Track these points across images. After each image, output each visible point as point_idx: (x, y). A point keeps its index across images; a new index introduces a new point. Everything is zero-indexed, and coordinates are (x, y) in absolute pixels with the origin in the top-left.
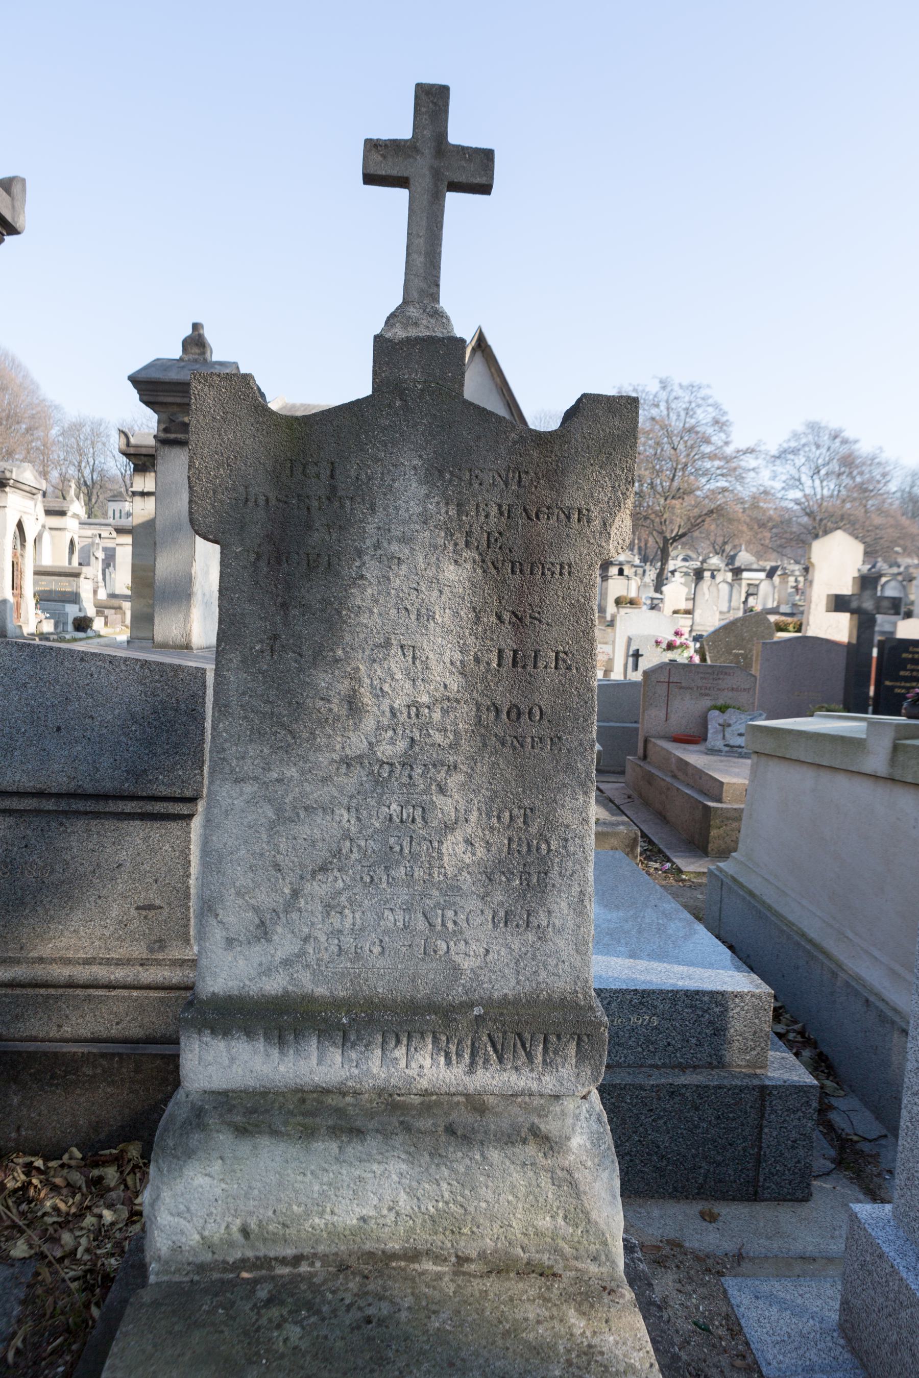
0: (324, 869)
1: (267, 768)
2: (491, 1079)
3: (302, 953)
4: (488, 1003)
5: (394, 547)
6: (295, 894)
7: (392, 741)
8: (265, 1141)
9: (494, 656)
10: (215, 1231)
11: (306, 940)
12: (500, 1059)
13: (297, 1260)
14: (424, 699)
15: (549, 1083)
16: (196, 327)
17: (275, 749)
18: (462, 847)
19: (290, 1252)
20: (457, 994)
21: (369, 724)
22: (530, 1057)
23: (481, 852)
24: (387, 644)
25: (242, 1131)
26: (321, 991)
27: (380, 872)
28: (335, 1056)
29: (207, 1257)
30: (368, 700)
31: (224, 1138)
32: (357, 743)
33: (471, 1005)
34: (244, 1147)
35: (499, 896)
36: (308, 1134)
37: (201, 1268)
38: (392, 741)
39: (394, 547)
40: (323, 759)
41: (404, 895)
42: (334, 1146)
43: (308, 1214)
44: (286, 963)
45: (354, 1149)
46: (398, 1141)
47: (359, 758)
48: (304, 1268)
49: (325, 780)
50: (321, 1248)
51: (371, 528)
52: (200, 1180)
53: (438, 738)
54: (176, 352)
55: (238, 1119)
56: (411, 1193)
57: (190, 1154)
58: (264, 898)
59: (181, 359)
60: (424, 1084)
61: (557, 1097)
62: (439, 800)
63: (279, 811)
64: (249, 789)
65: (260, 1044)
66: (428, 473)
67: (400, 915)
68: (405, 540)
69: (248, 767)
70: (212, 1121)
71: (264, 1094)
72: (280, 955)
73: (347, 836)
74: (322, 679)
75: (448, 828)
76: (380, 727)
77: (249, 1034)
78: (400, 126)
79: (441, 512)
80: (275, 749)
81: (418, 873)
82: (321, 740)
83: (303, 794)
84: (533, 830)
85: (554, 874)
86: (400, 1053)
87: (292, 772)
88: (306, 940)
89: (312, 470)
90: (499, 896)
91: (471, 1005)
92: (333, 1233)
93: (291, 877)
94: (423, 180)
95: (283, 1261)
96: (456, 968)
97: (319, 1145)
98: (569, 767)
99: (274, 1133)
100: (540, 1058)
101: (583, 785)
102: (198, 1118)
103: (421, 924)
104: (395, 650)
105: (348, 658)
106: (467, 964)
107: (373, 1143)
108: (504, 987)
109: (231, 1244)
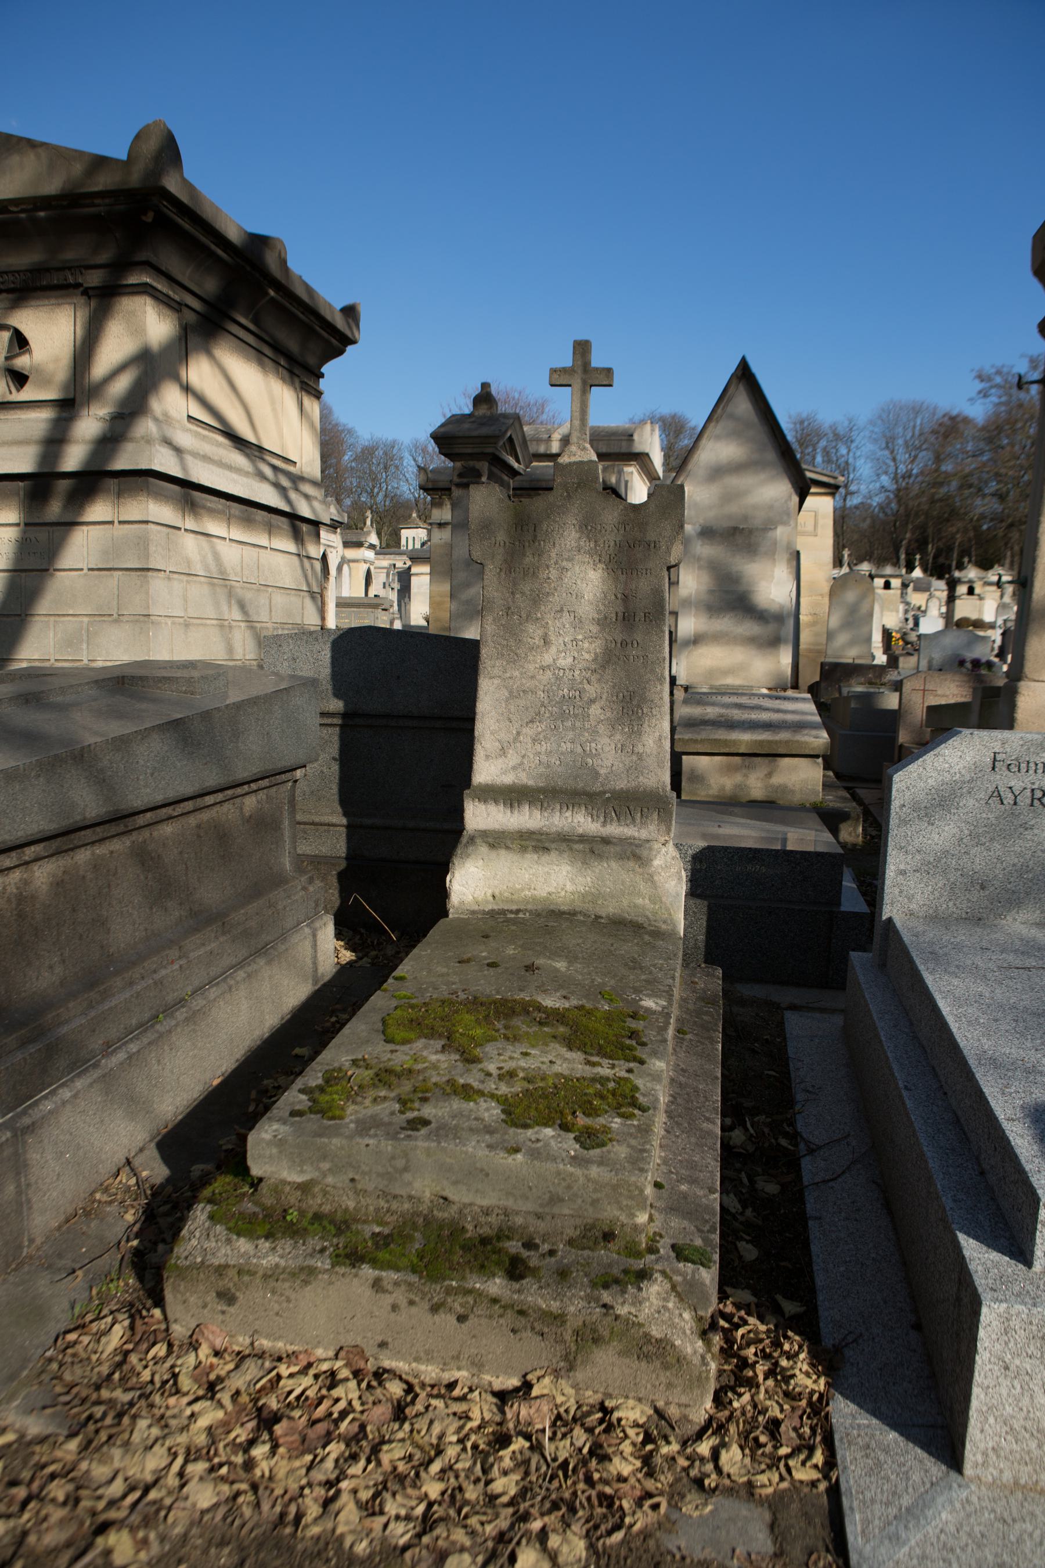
0: (532, 721)
1: (505, 672)
2: (614, 830)
3: (522, 763)
4: (613, 792)
5: (565, 563)
6: (518, 733)
7: (565, 658)
8: (503, 852)
9: (614, 615)
10: (480, 895)
11: (523, 757)
12: (619, 820)
13: (518, 911)
14: (580, 637)
15: (643, 834)
16: (485, 386)
17: (508, 662)
18: (600, 711)
19: (514, 907)
20: (597, 787)
21: (553, 650)
22: (633, 820)
23: (609, 714)
24: (562, 610)
25: (492, 846)
26: (531, 783)
27: (559, 723)
28: (537, 813)
29: (476, 908)
30: (553, 638)
31: (484, 849)
32: (547, 658)
33: (605, 793)
34: (493, 854)
35: (618, 737)
36: (524, 849)
37: (473, 912)
38: (565, 658)
39: (565, 563)
40: (531, 667)
41: (570, 735)
42: (535, 856)
43: (523, 890)
44: (514, 768)
45: (545, 858)
46: (565, 855)
47: (549, 666)
48: (521, 915)
49: (532, 677)
50: (529, 907)
51: (553, 555)
52: (472, 869)
53: (587, 656)
54: (467, 409)
55: (490, 840)
56: (572, 880)
57: (468, 856)
58: (503, 736)
59: (470, 415)
60: (580, 831)
61: (648, 841)
62: (587, 686)
63: (511, 692)
64: (496, 681)
65: (501, 807)
66: (580, 527)
67: (569, 745)
68: (570, 560)
69: (496, 671)
70: (478, 841)
71: (503, 832)
72: (511, 764)
73: (543, 705)
74: (531, 628)
75: (592, 701)
76: (559, 652)
77: (496, 802)
78: (566, 360)
79: (587, 545)
80: (508, 662)
81: (578, 724)
82: (531, 658)
83: (522, 685)
84: (635, 703)
85: (645, 725)
86: (568, 814)
87: (517, 673)
88: (523, 757)
89: (525, 528)
90: (618, 737)
91: (605, 793)
92: (534, 899)
93: (517, 725)
94: (577, 383)
95: (511, 912)
96: (597, 773)
97: (528, 856)
98: (653, 671)
99: (507, 848)
100: (638, 821)
101: (659, 680)
102: (472, 839)
103: (579, 750)
104: (565, 614)
105: (543, 619)
106: (603, 771)
107: (554, 854)
108: (621, 784)
109: (487, 902)
